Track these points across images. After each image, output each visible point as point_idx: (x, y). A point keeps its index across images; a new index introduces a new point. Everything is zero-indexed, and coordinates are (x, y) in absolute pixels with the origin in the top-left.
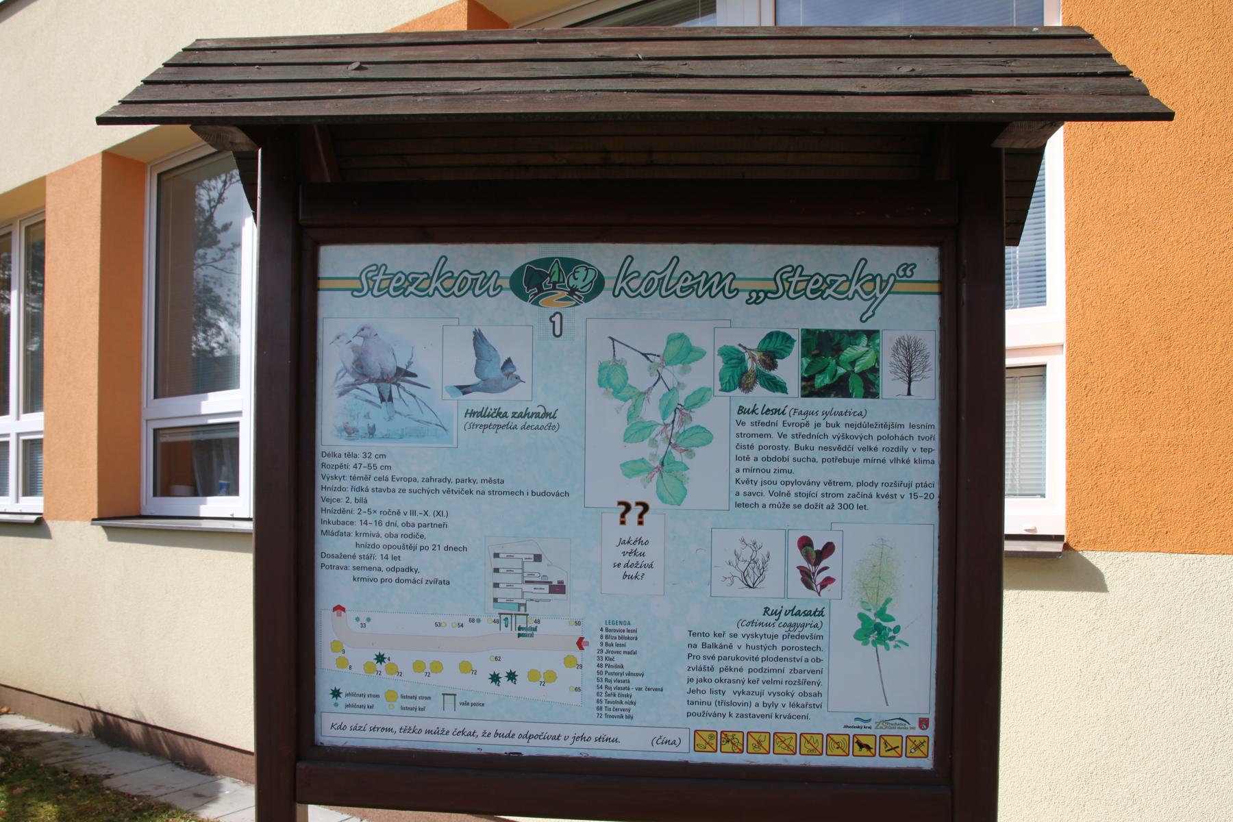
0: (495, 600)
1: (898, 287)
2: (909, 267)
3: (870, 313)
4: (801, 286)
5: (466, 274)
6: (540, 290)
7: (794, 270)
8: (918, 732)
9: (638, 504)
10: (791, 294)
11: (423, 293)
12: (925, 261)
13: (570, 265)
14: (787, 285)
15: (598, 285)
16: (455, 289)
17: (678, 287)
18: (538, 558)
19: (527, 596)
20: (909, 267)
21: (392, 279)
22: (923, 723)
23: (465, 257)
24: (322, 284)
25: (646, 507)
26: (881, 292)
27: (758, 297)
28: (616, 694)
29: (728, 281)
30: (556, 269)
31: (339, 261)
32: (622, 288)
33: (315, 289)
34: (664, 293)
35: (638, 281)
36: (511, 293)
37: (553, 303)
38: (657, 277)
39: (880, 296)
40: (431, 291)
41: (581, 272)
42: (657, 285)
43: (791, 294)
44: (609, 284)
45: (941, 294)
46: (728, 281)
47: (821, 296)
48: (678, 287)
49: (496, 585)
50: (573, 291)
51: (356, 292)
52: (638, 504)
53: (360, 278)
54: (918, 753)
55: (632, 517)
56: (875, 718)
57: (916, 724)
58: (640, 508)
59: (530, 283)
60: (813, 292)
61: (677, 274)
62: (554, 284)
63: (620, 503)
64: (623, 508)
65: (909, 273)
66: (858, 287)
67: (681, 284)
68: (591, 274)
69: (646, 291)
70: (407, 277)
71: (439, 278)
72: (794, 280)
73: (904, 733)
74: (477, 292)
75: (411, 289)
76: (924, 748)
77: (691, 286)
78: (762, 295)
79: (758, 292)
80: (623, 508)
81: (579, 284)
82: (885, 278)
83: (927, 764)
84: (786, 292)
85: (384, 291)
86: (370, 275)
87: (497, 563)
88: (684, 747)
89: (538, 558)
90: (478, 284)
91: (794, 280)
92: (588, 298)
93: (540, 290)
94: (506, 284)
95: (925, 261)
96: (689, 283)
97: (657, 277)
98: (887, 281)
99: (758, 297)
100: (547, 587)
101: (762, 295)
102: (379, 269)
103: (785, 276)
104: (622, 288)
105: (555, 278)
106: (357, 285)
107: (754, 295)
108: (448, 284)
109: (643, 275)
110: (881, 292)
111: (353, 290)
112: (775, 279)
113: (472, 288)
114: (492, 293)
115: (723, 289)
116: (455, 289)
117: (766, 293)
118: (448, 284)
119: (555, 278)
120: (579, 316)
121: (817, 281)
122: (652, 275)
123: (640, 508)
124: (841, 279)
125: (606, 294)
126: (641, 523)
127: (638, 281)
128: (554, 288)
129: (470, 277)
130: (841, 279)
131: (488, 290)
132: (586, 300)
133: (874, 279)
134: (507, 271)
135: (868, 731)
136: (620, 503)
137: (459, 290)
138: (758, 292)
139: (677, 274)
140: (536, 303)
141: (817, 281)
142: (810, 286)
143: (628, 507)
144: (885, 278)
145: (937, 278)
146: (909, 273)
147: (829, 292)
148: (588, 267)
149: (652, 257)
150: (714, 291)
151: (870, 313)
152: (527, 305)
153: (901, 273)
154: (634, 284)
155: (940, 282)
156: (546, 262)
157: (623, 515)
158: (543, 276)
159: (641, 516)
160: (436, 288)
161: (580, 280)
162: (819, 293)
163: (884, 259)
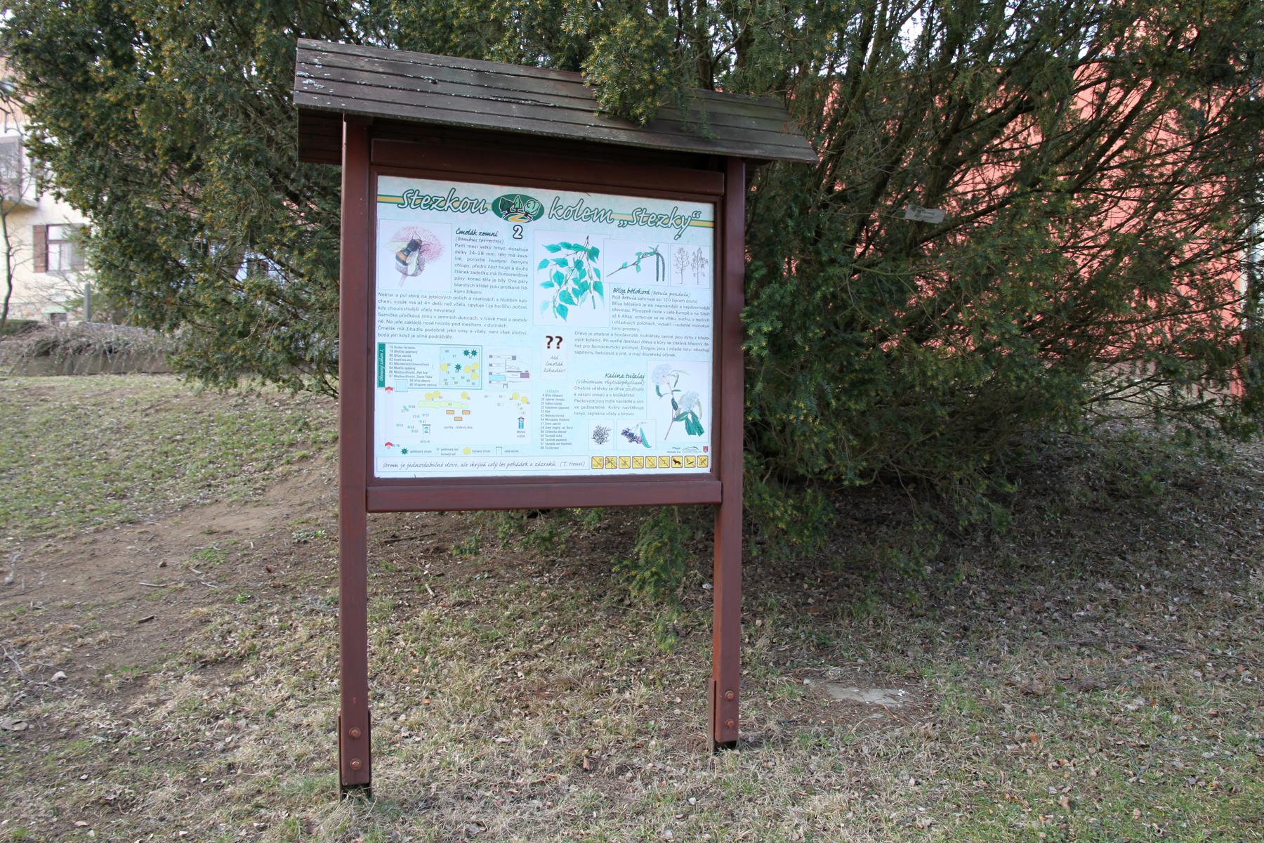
2: (697, 213)
12: (706, 211)
13: (525, 199)
15: (541, 211)
18: (514, 358)
20: (697, 213)
23: (466, 190)
24: (379, 199)
28: (554, 437)
37: (515, 220)
42: (571, 214)
44: (546, 211)
45: (715, 228)
50: (527, 214)
59: (503, 208)
81: (530, 210)
83: (707, 470)
89: (514, 358)
90: (473, 206)
92: (536, 218)
94: (490, 207)
95: (706, 211)
118: (456, 204)
120: (529, 227)
125: (545, 216)
134: (491, 200)
148: (535, 201)
149: (570, 198)
154: (560, 212)
155: (715, 222)
158: (511, 204)
162: (654, 223)
163: (686, 208)
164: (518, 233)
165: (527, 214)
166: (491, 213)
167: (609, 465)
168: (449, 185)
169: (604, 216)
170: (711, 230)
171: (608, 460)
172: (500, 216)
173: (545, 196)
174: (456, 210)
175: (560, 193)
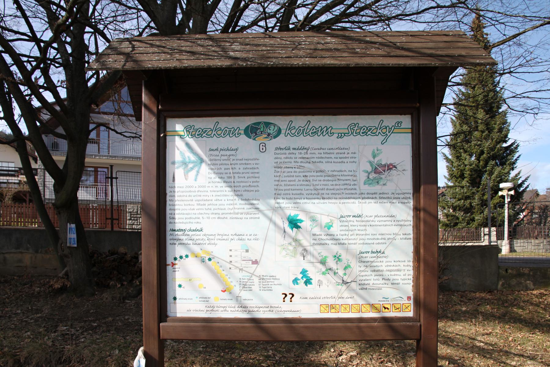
1: (395, 131)
3: (385, 141)
4: (358, 131)
5: (226, 129)
6: (256, 134)
7: (355, 125)
8: (407, 302)
10: (354, 134)
11: (210, 136)
12: (406, 121)
13: (267, 124)
14: (352, 131)
15: (279, 132)
16: (222, 134)
17: (310, 132)
19: (243, 266)
22: (409, 298)
23: (226, 122)
29: (329, 130)
30: (262, 126)
35: (295, 130)
36: (244, 136)
37: (261, 139)
38: (302, 129)
39: (389, 134)
40: (212, 135)
41: (272, 127)
42: (302, 132)
43: (354, 134)
44: (283, 132)
45: (412, 133)
46: (329, 130)
48: (310, 132)
50: (269, 135)
54: (407, 310)
57: (406, 298)
59: (252, 132)
61: (310, 127)
62: (262, 132)
65: (399, 125)
66: (380, 131)
67: (311, 131)
68: (276, 128)
70: (202, 130)
72: (355, 129)
73: (402, 303)
74: (231, 135)
75: (204, 135)
76: (409, 308)
77: (315, 132)
78: (343, 135)
81: (271, 132)
82: (390, 127)
83: (411, 314)
87: (231, 253)
90: (232, 133)
91: (355, 129)
92: (275, 137)
94: (242, 132)
95: (406, 121)
96: (314, 131)
97: (302, 129)
98: (391, 128)
100: (251, 262)
101: (343, 135)
105: (262, 130)
107: (340, 135)
108: (219, 132)
109: (297, 128)
110: (389, 132)
113: (229, 134)
114: (237, 136)
115: (328, 133)
116: (222, 134)
118: (219, 132)
119: (262, 130)
121: (364, 129)
124: (373, 128)
125: (282, 135)
127: (295, 130)
128: (262, 133)
129: (228, 130)
130: (373, 128)
133: (386, 128)
134: (243, 126)
135: (388, 302)
137: (224, 135)
139: (310, 127)
140: (254, 139)
141: (364, 129)
142: (362, 131)
144: (390, 127)
145: (410, 127)
146: (399, 125)
147: (369, 133)
148: (275, 125)
149: (299, 121)
150: (324, 134)
151: (385, 141)
153: (397, 125)
154: (293, 132)
155: (412, 128)
156: (259, 123)
158: (257, 129)
160: (214, 134)
161: (272, 130)
162: (365, 133)
163: (390, 120)
164: (263, 149)
166: (243, 137)
167: (333, 310)
170: (410, 134)
172: (250, 137)
173: (281, 122)
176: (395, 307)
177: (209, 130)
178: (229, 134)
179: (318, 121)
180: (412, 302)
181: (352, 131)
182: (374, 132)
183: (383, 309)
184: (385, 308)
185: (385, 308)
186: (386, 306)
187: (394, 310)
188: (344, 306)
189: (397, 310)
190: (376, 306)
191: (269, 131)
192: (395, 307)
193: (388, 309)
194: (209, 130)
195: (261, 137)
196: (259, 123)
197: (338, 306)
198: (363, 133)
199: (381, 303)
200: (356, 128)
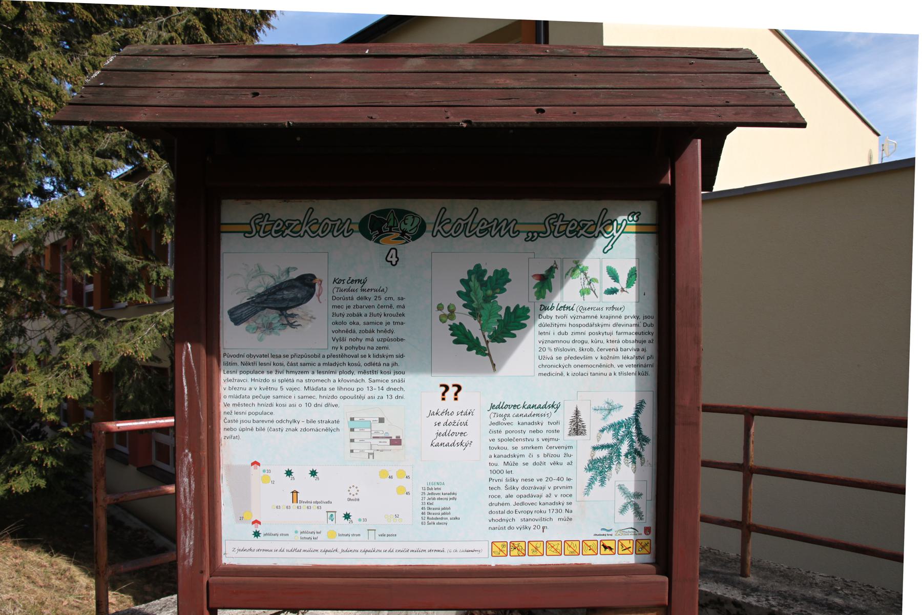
0: (352, 451)
3: (610, 247)
4: (563, 228)
5: (327, 221)
6: (381, 232)
7: (558, 217)
9: (454, 385)
11: (296, 234)
13: (401, 214)
14: (553, 228)
17: (478, 230)
18: (381, 420)
21: (273, 224)
23: (326, 209)
24: (223, 228)
25: (459, 388)
26: (617, 232)
27: (533, 237)
29: (512, 225)
30: (392, 217)
31: (234, 212)
32: (438, 231)
33: (220, 232)
34: (468, 234)
36: (359, 235)
38: (463, 223)
39: (616, 235)
43: (556, 234)
44: (429, 228)
47: (576, 235)
48: (478, 230)
49: (352, 441)
50: (404, 233)
51: (248, 234)
52: (454, 385)
53: (250, 224)
55: (450, 394)
56: (615, 528)
58: (456, 389)
59: (373, 228)
60: (570, 232)
61: (476, 221)
62: (391, 227)
63: (441, 386)
64: (443, 389)
67: (479, 227)
68: (417, 221)
69: (455, 232)
71: (308, 223)
72: (558, 224)
74: (336, 234)
75: (287, 232)
77: (487, 229)
78: (535, 235)
79: (533, 233)
80: (443, 389)
81: (408, 228)
84: (552, 232)
85: (267, 233)
86: (257, 221)
88: (486, 551)
89: (381, 420)
90: (338, 228)
92: (415, 238)
93: (381, 232)
94: (356, 227)
96: (485, 227)
97: (463, 223)
99: (533, 237)
101: (535, 235)
102: (264, 217)
103: (551, 221)
104: (438, 231)
105: (391, 224)
106: (248, 228)
107: (530, 235)
109: (453, 221)
110: (617, 232)
111: (245, 233)
112: (544, 223)
113: (332, 231)
114: (346, 234)
117: (538, 234)
118: (314, 228)
119: (391, 224)
121: (573, 225)
122: (460, 221)
123: (456, 389)
125: (427, 235)
126: (456, 399)
128: (390, 231)
129: (330, 223)
131: (343, 232)
132: (413, 239)
134: (357, 218)
136: (441, 386)
137: (323, 232)
138: (533, 233)
139: (476, 221)
140: (377, 241)
141: (573, 225)
142: (569, 228)
143: (447, 388)
147: (582, 232)
148: (414, 215)
149: (460, 208)
150: (503, 233)
151: (610, 247)
152: (372, 242)
156: (384, 212)
157: (443, 394)
158: (383, 222)
159: (456, 394)
160: (306, 231)
161: (409, 225)
165: (404, 233)
166: (358, 237)
167: (515, 552)
168: (305, 205)
169: (507, 228)
171: (514, 546)
172: (369, 238)
173: (426, 209)
174: (315, 234)
175: (446, 203)
176: (622, 545)
177: (295, 223)
178: (332, 231)
179: (489, 209)
180: (651, 536)
181: (553, 228)
182: (590, 230)
183: (603, 548)
184: (606, 547)
185: (606, 547)
186: (607, 544)
187: (620, 552)
188: (534, 544)
189: (627, 552)
190: (589, 543)
191: (403, 226)
192: (622, 545)
193: (610, 548)
194: (295, 223)
195: (390, 238)
196: (387, 211)
197: (522, 544)
198: (570, 232)
199: (599, 538)
200: (560, 223)
